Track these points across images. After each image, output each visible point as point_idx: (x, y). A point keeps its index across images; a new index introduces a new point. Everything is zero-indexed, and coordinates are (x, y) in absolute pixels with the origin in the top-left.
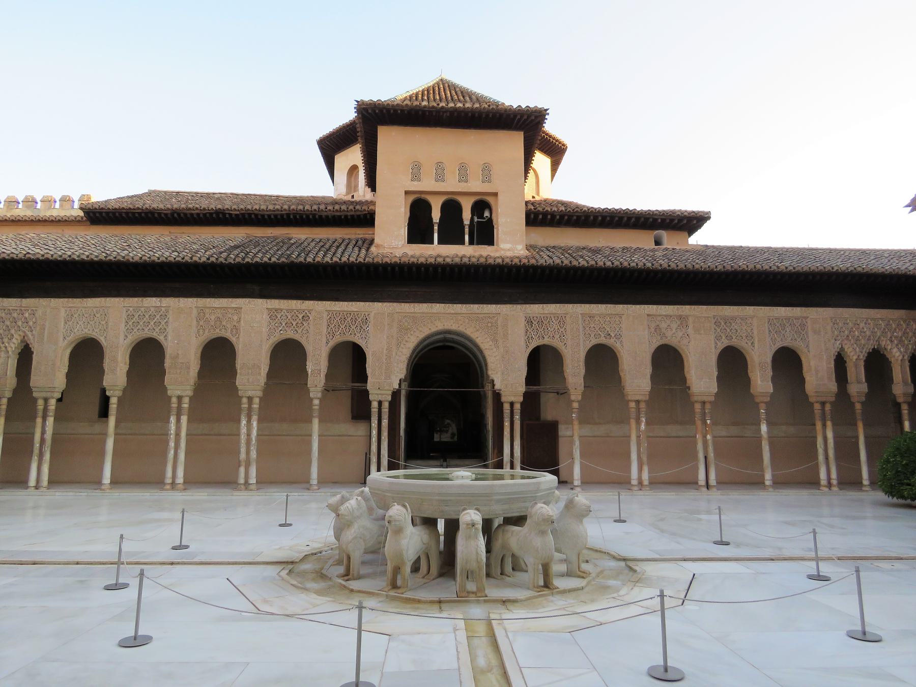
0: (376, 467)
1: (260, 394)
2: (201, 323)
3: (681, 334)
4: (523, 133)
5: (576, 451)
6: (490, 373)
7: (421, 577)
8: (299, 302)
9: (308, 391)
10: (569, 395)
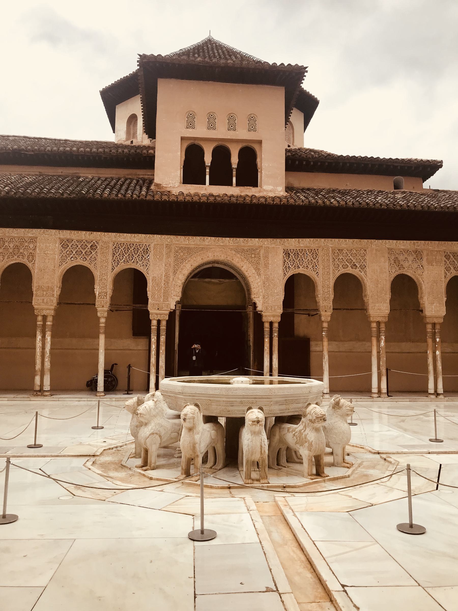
1: (52, 313)
3: (416, 265)
5: (325, 363)
6: (253, 296)
7: (209, 467)
8: (88, 233)
9: (96, 311)
10: (320, 316)
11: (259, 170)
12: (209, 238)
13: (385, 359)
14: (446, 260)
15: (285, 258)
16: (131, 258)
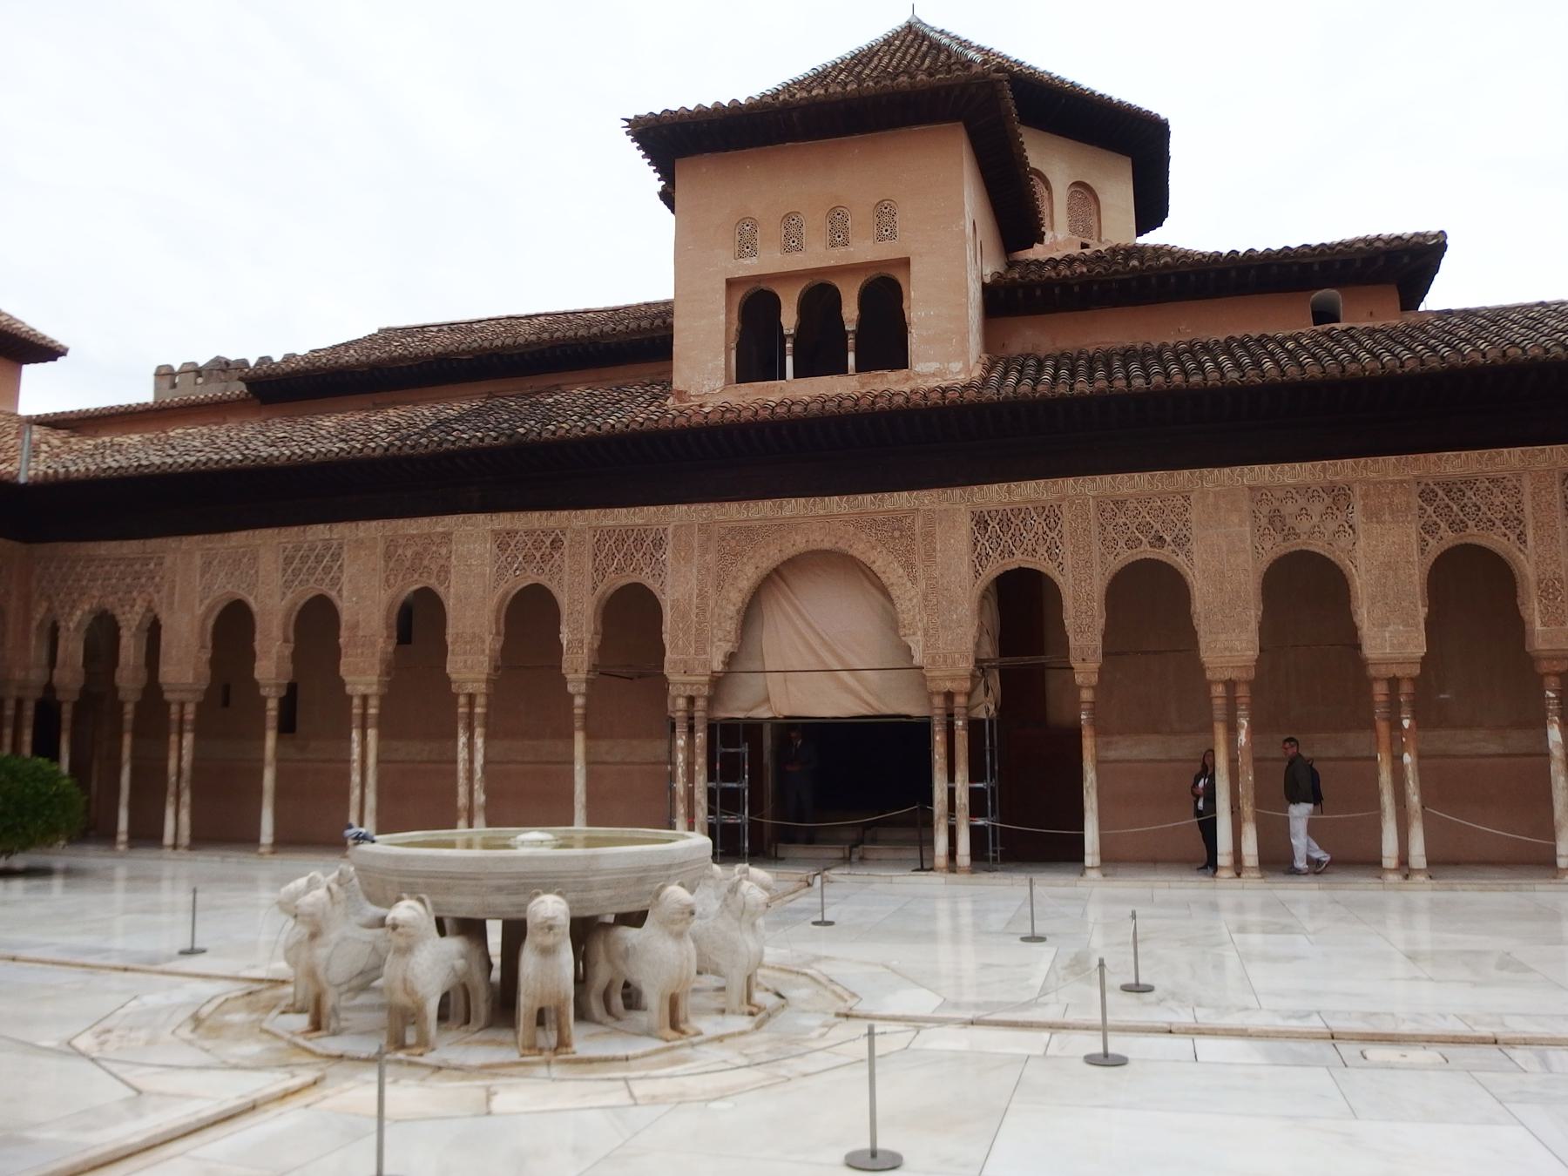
8: (545, 513)
9: (563, 681)
13: (1250, 778)
14: (1424, 505)
15: (977, 534)
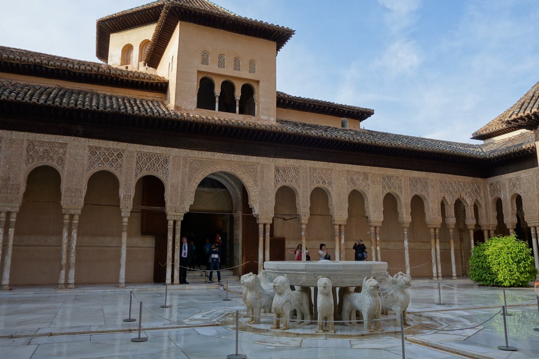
0: (171, 270)
1: (79, 212)
2: (31, 153)
4: (276, 43)
5: (304, 257)
8: (115, 143)
11: (256, 103)
12: (218, 153)
16: (152, 167)
